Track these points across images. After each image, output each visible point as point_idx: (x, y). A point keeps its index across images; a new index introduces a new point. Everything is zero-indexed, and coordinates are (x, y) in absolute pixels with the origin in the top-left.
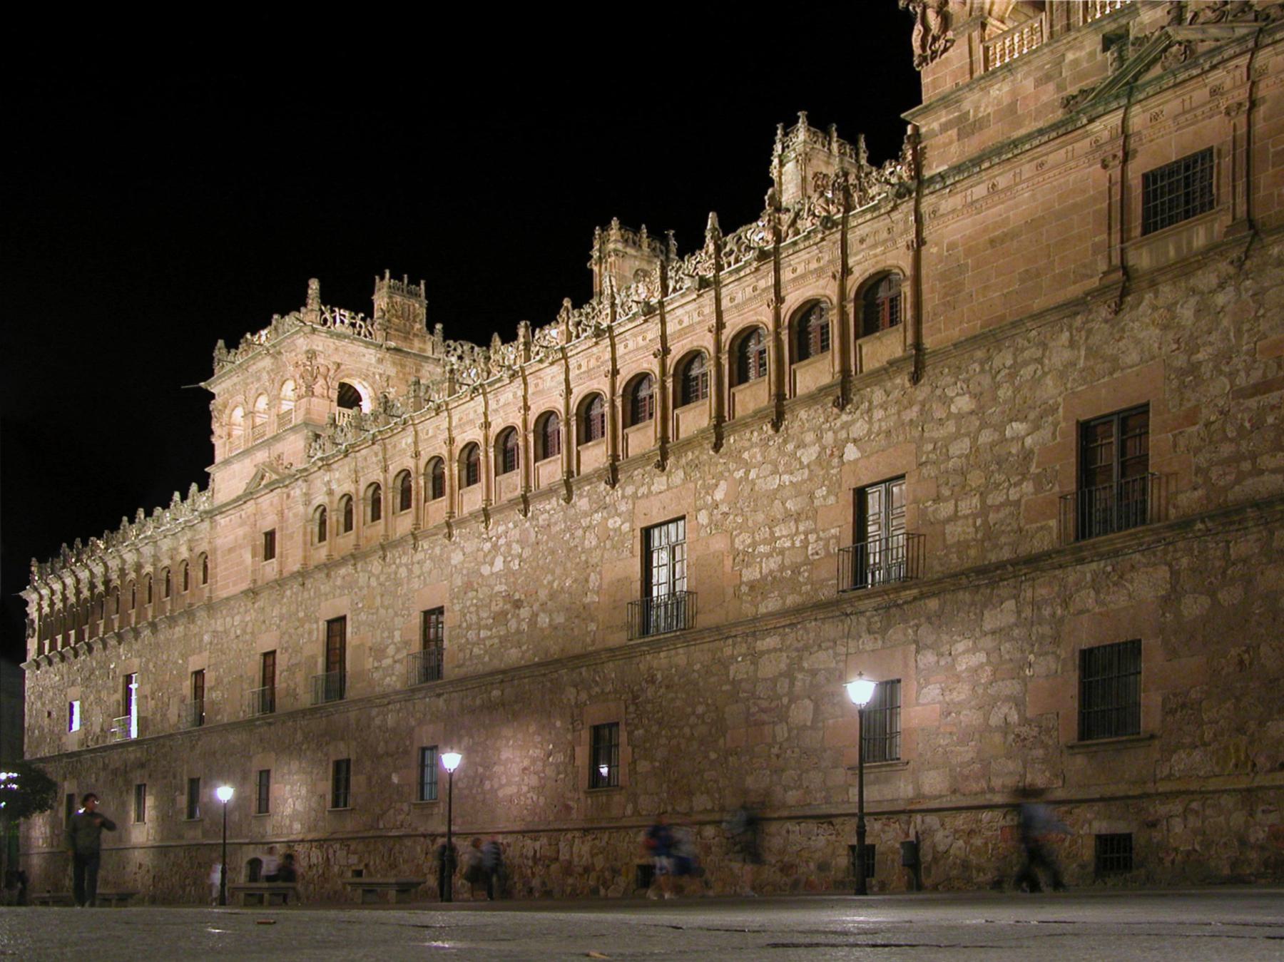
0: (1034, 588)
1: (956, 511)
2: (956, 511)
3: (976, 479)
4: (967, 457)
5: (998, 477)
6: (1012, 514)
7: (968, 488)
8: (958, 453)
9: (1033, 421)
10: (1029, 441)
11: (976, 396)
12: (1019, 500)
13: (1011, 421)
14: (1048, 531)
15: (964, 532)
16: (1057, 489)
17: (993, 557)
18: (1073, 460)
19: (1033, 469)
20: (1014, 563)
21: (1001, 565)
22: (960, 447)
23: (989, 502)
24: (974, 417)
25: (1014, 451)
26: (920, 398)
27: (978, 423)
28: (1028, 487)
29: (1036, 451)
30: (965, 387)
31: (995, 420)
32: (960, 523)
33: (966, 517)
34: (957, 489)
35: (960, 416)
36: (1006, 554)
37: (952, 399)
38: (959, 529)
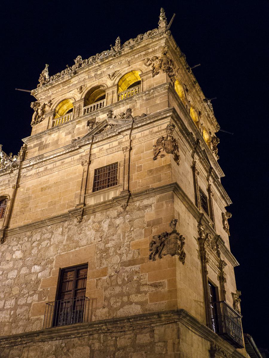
0: (28, 351)
1: (4, 306)
2: (4, 306)
3: (16, 291)
4: (14, 279)
5: (26, 291)
6: (27, 310)
7: (11, 295)
8: (11, 277)
9: (43, 266)
10: (40, 275)
11: (24, 252)
12: (31, 304)
13: (35, 265)
14: (40, 321)
15: (5, 317)
16: (47, 300)
17: (14, 332)
18: (56, 286)
19: (40, 289)
20: (21, 336)
21: (16, 337)
22: (13, 274)
23: (19, 303)
24: (21, 261)
25: (33, 279)
26: (2, 250)
27: (22, 264)
28: (36, 297)
29: (42, 280)
30: (20, 247)
31: (29, 263)
32: (4, 312)
33: (7, 309)
34: (7, 294)
35: (16, 260)
36: (20, 331)
37: (14, 251)
38: (3, 316)
